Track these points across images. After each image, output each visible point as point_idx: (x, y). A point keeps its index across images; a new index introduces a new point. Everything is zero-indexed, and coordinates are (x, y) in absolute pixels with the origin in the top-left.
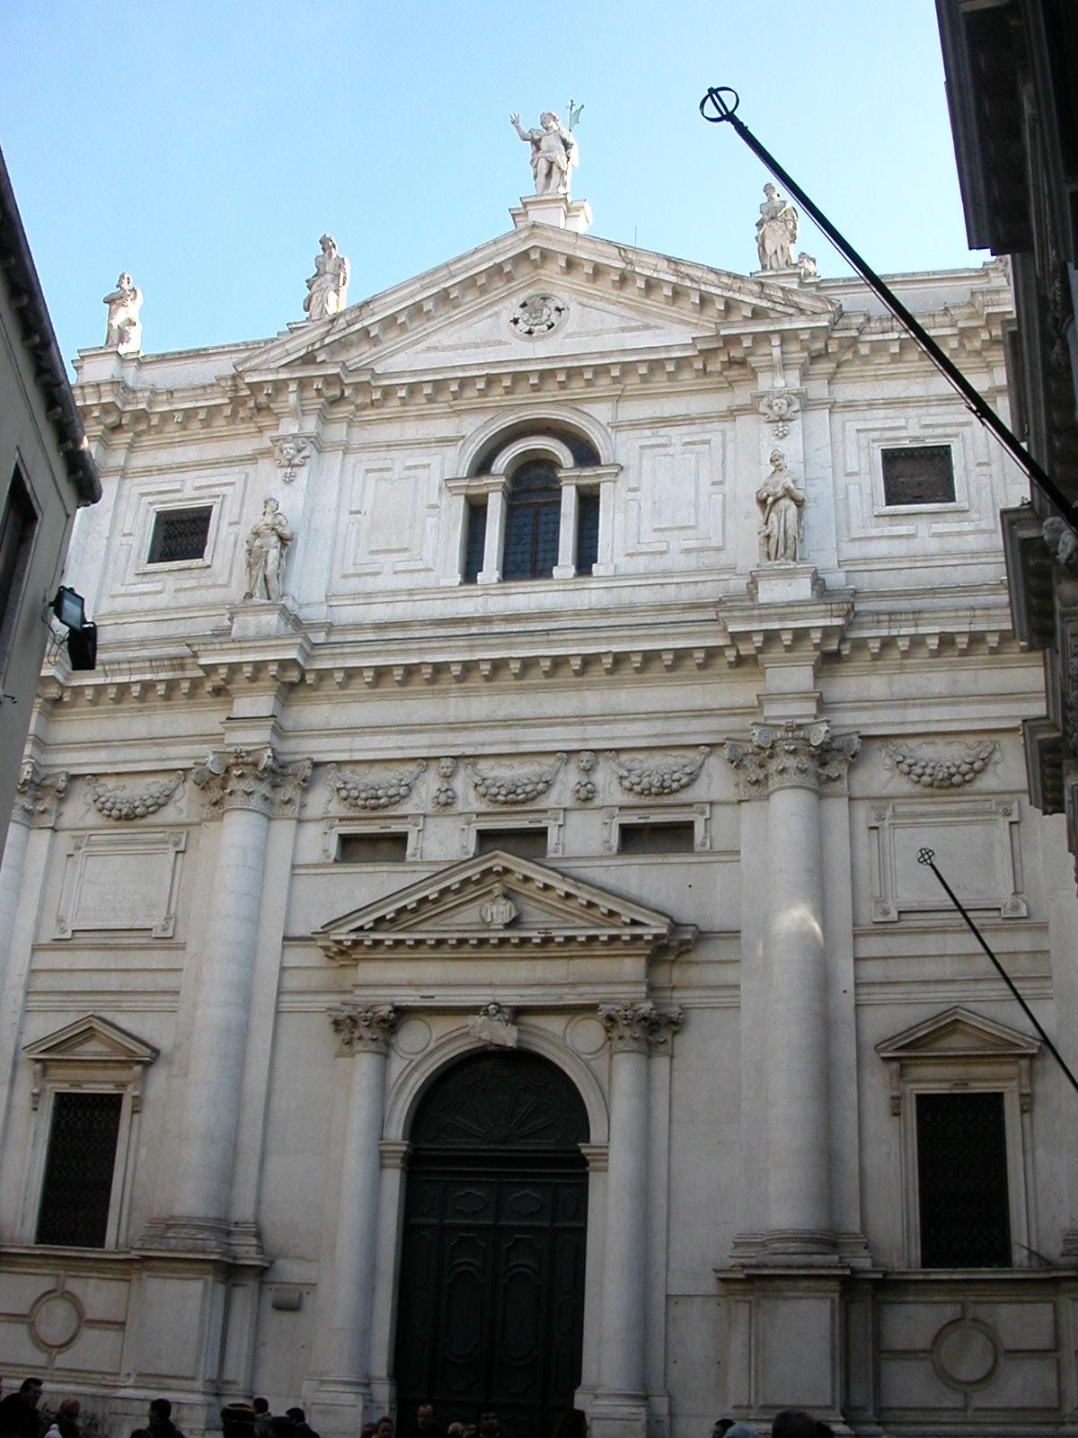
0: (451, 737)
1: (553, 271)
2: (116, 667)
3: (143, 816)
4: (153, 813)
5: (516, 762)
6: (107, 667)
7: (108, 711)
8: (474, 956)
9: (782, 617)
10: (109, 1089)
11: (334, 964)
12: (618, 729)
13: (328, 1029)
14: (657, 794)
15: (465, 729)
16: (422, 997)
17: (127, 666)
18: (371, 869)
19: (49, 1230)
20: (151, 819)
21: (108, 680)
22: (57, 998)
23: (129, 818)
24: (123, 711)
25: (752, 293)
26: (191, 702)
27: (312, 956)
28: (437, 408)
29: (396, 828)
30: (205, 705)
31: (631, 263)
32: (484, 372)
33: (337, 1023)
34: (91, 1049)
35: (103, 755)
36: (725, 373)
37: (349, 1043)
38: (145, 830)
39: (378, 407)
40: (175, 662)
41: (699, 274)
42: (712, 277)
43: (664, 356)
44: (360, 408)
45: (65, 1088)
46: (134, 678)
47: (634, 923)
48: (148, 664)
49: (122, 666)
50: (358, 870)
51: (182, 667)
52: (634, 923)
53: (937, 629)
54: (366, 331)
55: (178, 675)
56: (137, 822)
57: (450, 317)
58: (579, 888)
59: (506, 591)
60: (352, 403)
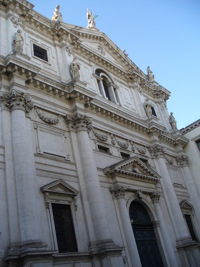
0: (112, 130)
1: (102, 43)
2: (48, 80)
3: (53, 124)
4: (55, 124)
5: (121, 139)
6: (46, 79)
7: (38, 91)
8: (134, 179)
9: (159, 127)
10: (66, 203)
11: (106, 176)
12: (135, 139)
13: (109, 193)
14: (142, 153)
15: (114, 129)
16: (128, 186)
17: (51, 81)
18: (106, 155)
19: (62, 249)
20: (54, 126)
21: (45, 82)
22: (44, 172)
23: (49, 123)
24: (42, 92)
25: (136, 68)
26: (60, 98)
27: (102, 173)
28: (87, 57)
29: (107, 147)
30: (62, 100)
31: (118, 51)
32: (98, 56)
33: (111, 192)
34: (59, 190)
35: (40, 102)
36: (129, 79)
37: (117, 196)
38: (53, 128)
39: (77, 50)
40: (63, 86)
41: (129, 60)
42: (131, 61)
43: (123, 71)
44: (75, 48)
45: (54, 202)
46: (52, 85)
47: (156, 177)
48: (56, 83)
49: (50, 80)
50: (103, 154)
51: (64, 88)
52: (156, 177)
53: (168, 137)
54: (79, 33)
55: (63, 90)
56: (51, 125)
57: (88, 40)
58: (148, 168)
59: (109, 102)
60: (74, 46)
